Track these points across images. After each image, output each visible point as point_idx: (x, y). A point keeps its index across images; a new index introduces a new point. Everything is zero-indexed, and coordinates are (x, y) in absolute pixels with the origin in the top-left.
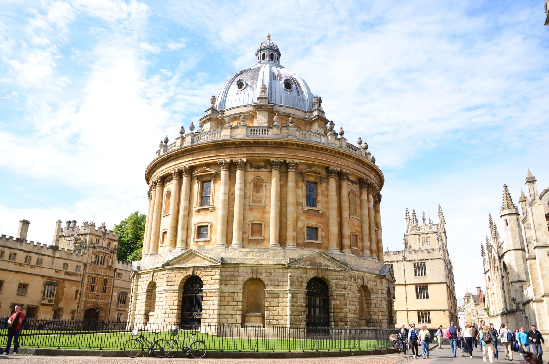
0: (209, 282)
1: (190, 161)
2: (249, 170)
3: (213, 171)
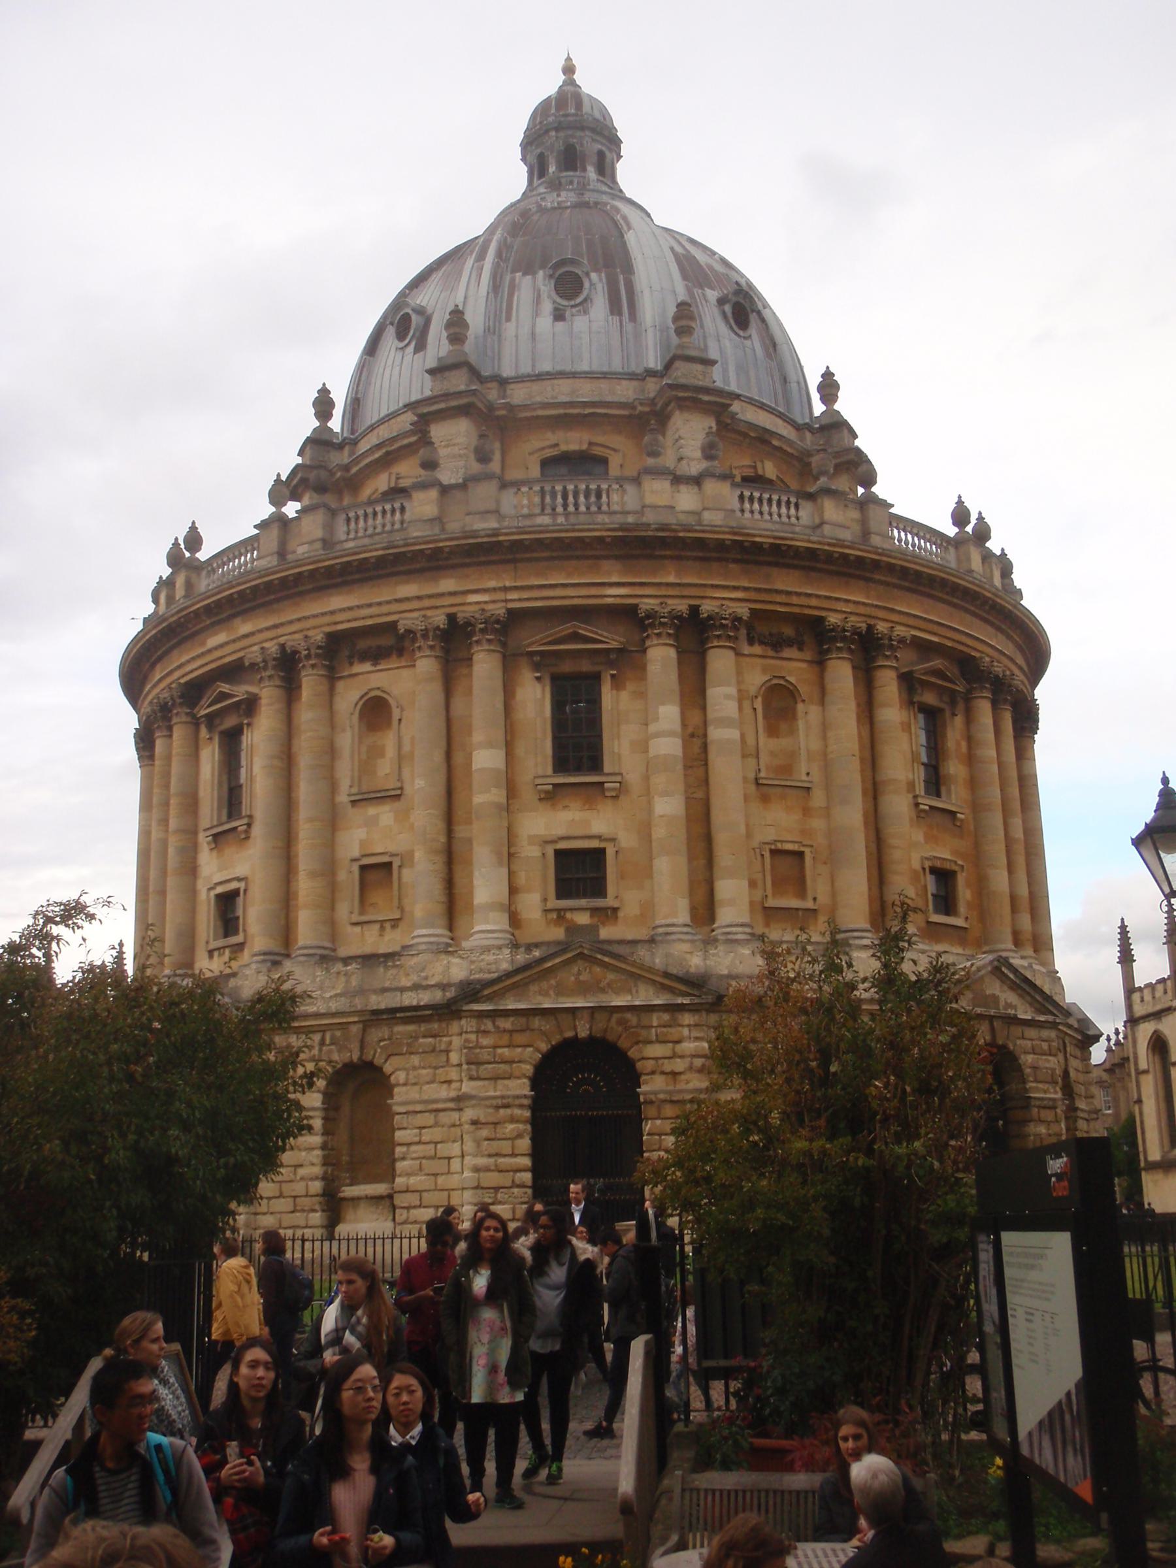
0: (668, 1066)
1: (506, 589)
2: (747, 649)
3: (611, 638)
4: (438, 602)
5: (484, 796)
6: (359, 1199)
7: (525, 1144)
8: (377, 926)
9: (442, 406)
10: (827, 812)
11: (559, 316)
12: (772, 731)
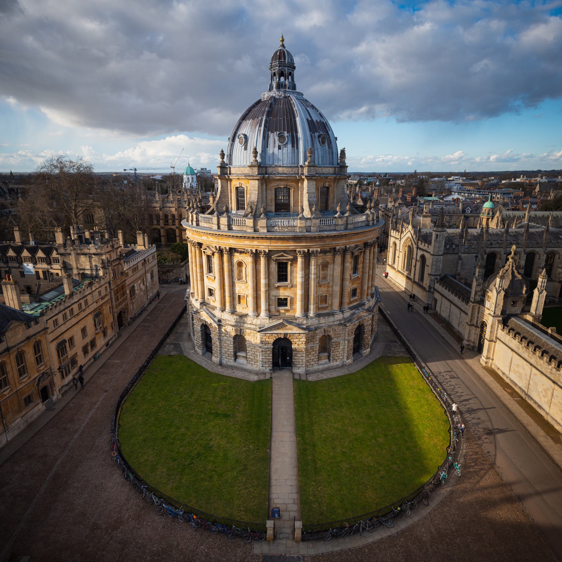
5: (263, 289)
6: (240, 356)
7: (271, 355)
10: (332, 286)
11: (279, 148)
12: (323, 270)
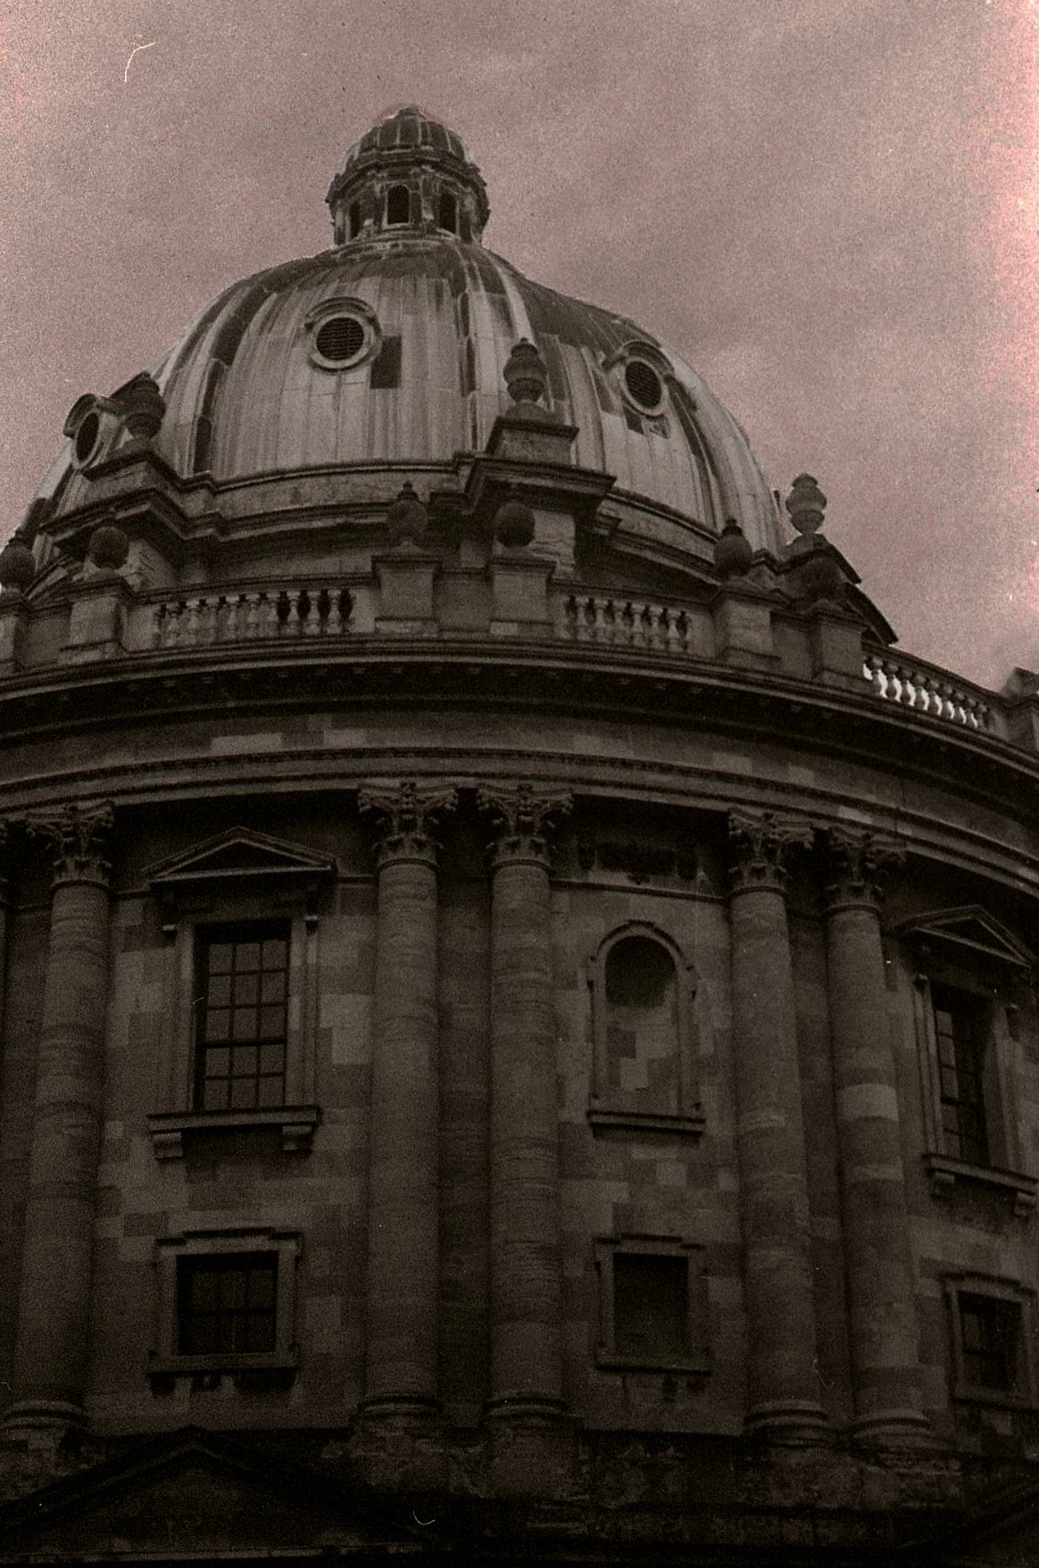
1: (898, 816)
4: (791, 801)
8: (659, 1381)
9: (549, 483)
